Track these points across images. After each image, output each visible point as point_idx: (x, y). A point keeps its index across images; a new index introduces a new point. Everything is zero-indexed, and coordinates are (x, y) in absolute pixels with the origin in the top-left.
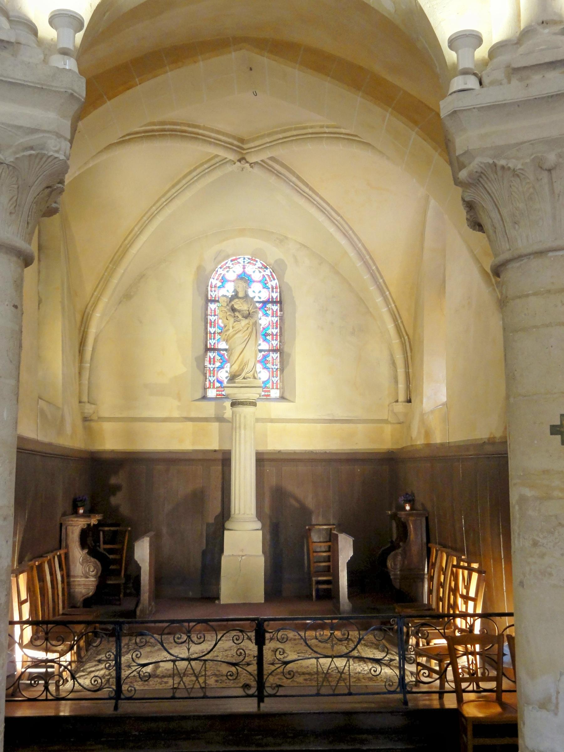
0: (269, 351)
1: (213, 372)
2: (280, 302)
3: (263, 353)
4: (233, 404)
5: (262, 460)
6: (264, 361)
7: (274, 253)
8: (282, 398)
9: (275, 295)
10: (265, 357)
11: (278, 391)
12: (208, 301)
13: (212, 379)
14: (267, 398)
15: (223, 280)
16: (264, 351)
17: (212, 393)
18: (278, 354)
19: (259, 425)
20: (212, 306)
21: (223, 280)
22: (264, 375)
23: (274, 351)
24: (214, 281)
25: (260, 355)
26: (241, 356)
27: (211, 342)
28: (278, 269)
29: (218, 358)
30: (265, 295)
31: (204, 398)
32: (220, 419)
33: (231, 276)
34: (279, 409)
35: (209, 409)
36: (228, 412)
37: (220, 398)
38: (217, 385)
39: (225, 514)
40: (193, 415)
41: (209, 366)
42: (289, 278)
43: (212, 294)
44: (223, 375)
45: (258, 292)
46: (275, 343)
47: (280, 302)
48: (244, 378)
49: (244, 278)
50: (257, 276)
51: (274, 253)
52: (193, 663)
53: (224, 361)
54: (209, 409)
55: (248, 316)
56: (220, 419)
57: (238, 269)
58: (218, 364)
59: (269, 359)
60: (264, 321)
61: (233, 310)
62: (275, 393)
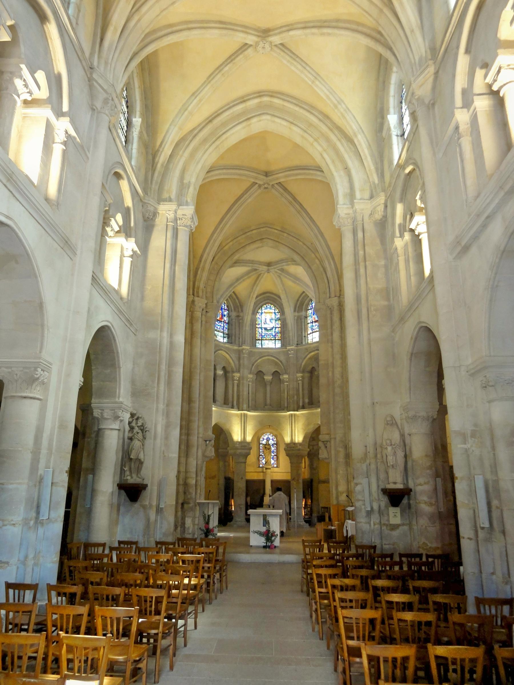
2: (276, 444)
4: (266, 469)
5: (272, 481)
6: (273, 458)
7: (275, 433)
8: (277, 467)
9: (275, 442)
12: (260, 444)
14: (274, 467)
15: (264, 439)
17: (261, 466)
19: (272, 474)
20: (261, 445)
21: (264, 439)
22: (272, 462)
24: (261, 439)
27: (261, 454)
28: (276, 436)
30: (273, 442)
31: (259, 467)
32: (263, 472)
33: (265, 438)
34: (276, 470)
35: (260, 470)
36: (265, 470)
37: (262, 467)
39: (264, 494)
40: (257, 471)
42: (278, 439)
43: (261, 442)
44: (264, 461)
45: (271, 442)
46: (275, 454)
47: (276, 444)
49: (268, 440)
50: (271, 438)
51: (275, 433)
53: (263, 458)
54: (260, 470)
55: (269, 449)
56: (263, 472)
57: (267, 436)
60: (273, 449)
61: (266, 448)
62: (275, 466)
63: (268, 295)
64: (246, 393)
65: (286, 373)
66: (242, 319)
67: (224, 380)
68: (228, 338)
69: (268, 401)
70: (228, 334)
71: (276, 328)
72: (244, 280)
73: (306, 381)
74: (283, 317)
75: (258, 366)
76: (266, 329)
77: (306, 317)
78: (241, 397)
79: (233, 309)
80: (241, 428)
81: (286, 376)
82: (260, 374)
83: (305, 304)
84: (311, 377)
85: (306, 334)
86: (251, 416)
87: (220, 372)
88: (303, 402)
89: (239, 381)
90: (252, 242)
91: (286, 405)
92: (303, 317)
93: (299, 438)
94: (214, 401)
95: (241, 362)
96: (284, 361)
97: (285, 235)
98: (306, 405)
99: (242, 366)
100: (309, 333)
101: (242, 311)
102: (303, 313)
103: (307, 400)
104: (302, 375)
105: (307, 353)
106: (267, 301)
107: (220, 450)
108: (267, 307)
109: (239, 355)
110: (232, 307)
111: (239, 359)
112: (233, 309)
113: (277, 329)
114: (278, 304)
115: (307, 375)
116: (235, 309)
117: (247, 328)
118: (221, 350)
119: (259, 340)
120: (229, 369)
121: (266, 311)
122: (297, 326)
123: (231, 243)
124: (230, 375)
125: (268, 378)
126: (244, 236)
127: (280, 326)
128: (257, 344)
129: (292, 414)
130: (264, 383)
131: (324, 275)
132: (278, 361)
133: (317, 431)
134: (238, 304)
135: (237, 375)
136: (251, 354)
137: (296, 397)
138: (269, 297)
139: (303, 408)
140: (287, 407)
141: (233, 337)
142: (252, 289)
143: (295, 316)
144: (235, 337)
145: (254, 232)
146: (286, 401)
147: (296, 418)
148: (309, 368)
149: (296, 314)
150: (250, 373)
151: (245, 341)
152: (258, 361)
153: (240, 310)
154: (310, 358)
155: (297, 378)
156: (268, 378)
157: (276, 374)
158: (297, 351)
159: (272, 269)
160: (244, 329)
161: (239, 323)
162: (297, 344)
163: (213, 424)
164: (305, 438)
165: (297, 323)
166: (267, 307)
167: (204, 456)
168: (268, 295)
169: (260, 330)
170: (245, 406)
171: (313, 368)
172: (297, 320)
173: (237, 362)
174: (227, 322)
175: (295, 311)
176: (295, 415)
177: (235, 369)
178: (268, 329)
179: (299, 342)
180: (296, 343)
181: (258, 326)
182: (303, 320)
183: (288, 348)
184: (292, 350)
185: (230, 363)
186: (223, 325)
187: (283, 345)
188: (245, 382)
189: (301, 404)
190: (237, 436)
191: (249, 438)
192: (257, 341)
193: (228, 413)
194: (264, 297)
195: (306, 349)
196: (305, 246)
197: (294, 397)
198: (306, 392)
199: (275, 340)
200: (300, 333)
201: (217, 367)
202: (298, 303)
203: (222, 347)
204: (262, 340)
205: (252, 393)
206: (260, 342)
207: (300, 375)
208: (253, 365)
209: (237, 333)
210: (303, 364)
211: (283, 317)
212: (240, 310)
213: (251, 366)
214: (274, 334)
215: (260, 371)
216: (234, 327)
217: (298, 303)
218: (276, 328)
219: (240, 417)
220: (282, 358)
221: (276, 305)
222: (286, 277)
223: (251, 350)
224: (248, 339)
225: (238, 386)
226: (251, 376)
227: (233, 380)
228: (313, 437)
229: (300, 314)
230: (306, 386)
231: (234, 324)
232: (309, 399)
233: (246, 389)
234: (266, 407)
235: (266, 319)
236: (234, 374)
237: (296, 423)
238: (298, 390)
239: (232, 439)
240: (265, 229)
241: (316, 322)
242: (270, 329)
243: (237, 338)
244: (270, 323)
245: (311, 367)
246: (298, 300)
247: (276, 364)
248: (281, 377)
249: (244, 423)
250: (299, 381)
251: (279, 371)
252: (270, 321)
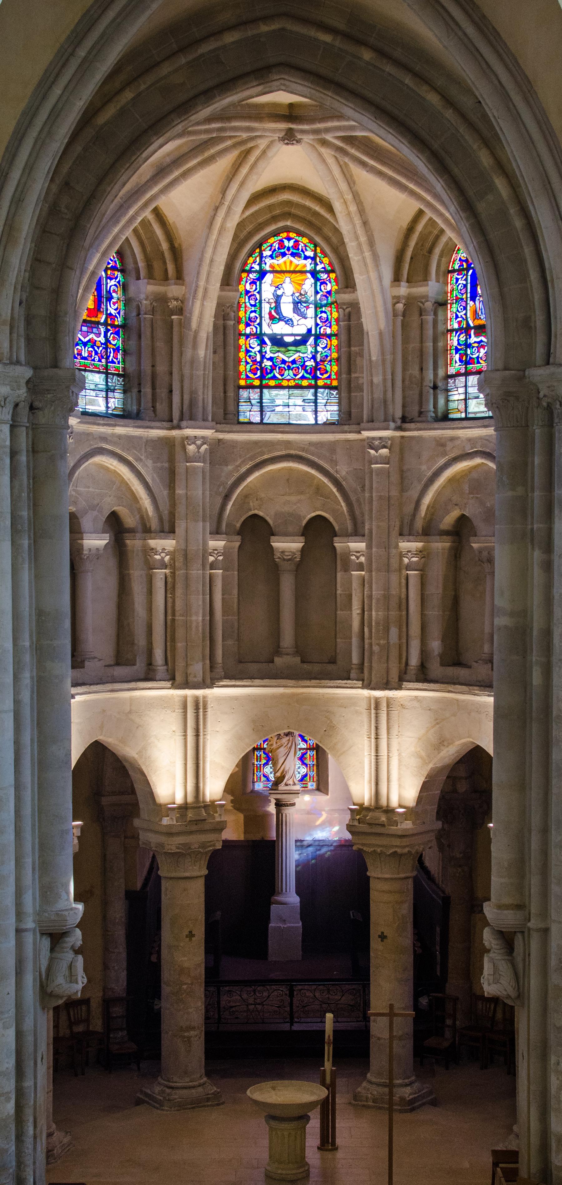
0: (307, 749)
1: (259, 768)
3: (302, 751)
10: (303, 754)
11: (315, 784)
13: (259, 774)
16: (303, 749)
18: (315, 752)
23: (310, 749)
25: (299, 754)
26: (283, 766)
29: (263, 756)
38: (263, 779)
41: (256, 763)
48: (286, 785)
52: (257, 1006)
58: (264, 761)
59: (307, 756)
63: (286, 196)
64: (198, 618)
65: (357, 533)
66: (180, 311)
67: (112, 563)
68: (125, 392)
69: (288, 639)
70: (124, 375)
71: (318, 337)
72: (185, 175)
73: (438, 570)
74: (346, 297)
75: (245, 497)
76: (278, 341)
77: (442, 304)
78: (180, 633)
79: (141, 265)
80: (183, 747)
81: (358, 545)
82: (255, 531)
83: (437, 251)
84: (456, 554)
85: (441, 373)
86: (220, 700)
87: (96, 542)
88: (424, 654)
89: (172, 566)
90: (217, 86)
91: (355, 659)
92: (429, 305)
93: (404, 789)
94: (77, 663)
95: (180, 491)
96: (349, 484)
97: (367, 55)
98: (435, 668)
99: (181, 510)
100: (452, 371)
101: (179, 276)
102: (431, 289)
103: (436, 645)
104: (420, 545)
105: (442, 461)
106: (281, 224)
107: (105, 801)
108: (281, 245)
109: (172, 460)
110: (139, 256)
111: (171, 477)
112: (141, 265)
113: (323, 343)
114: (327, 239)
115: (441, 546)
116: (150, 267)
117: (201, 353)
118: (101, 451)
119: (251, 387)
120: (130, 520)
121: (280, 262)
122: (406, 340)
123: (128, 95)
124: (133, 543)
125: (288, 546)
126: (183, 60)
127: (335, 328)
128: (243, 407)
129: (377, 703)
130: (272, 566)
131: (528, 251)
132: (325, 480)
133: (474, 760)
134: (165, 246)
135: (164, 546)
136: (218, 453)
137: (394, 632)
138: (289, 203)
139: (424, 676)
140: (362, 663)
141: (147, 390)
142: (224, 192)
143: (397, 299)
144: (154, 388)
145: (230, 38)
146: (355, 641)
147: (394, 714)
148: (449, 520)
149: (403, 290)
150: (216, 532)
151: (192, 403)
152: (250, 479)
153: (171, 268)
154: (451, 480)
155: (401, 556)
156: (288, 546)
157: (318, 531)
158: (401, 449)
159: (303, 132)
160: (188, 353)
161: (170, 325)
162: (404, 419)
163: (76, 750)
164: (425, 787)
165: (405, 326)
166: (281, 245)
167: (45, 992)
168: (286, 196)
169: (254, 343)
170: (197, 669)
171: (463, 520)
172: (404, 315)
173: (162, 493)
174: (119, 321)
175: (397, 279)
176: (389, 702)
177: (154, 524)
178: (288, 339)
179: (414, 410)
180: (399, 414)
181: (248, 330)
182: (430, 318)
183: (366, 434)
184: (383, 443)
185: (135, 498)
186: (102, 339)
187: (348, 418)
188: (196, 572)
189: (414, 661)
190: (168, 782)
191: (214, 787)
192: (244, 394)
193: (131, 699)
194: (270, 207)
195: (441, 443)
196: (449, 114)
197: (387, 630)
198: (435, 613)
199: (316, 387)
200: (416, 372)
201: (86, 523)
202: (412, 243)
203: (104, 438)
204: (261, 387)
205: (225, 612)
206: (254, 395)
207: (416, 545)
208: (227, 497)
209: (161, 368)
210: (427, 500)
211: (346, 297)
212: (171, 268)
213: (219, 500)
214: (310, 364)
215: (255, 516)
216: (146, 342)
217: (412, 243)
218: (318, 337)
219: (179, 711)
220: (342, 470)
221: (318, 239)
222: (364, 164)
223: (221, 436)
224: (206, 396)
225: (170, 587)
226: (217, 544)
227: (150, 566)
228: (461, 791)
229: (419, 290)
230: (436, 589)
231: (146, 332)
232: (444, 639)
233: (198, 602)
234: (277, 659)
235: (278, 299)
236: (152, 543)
237: (394, 731)
238: (404, 604)
239: (151, 794)
240: (275, 26)
241: (480, 329)
242: (296, 343)
243: (162, 393)
244: (295, 318)
245: (455, 514)
246: (410, 230)
247: (319, 490)
248: (339, 544)
249: (197, 736)
250: (408, 567)
251: (331, 520)
252: (296, 310)
